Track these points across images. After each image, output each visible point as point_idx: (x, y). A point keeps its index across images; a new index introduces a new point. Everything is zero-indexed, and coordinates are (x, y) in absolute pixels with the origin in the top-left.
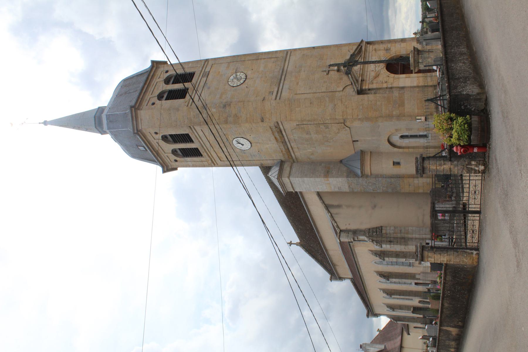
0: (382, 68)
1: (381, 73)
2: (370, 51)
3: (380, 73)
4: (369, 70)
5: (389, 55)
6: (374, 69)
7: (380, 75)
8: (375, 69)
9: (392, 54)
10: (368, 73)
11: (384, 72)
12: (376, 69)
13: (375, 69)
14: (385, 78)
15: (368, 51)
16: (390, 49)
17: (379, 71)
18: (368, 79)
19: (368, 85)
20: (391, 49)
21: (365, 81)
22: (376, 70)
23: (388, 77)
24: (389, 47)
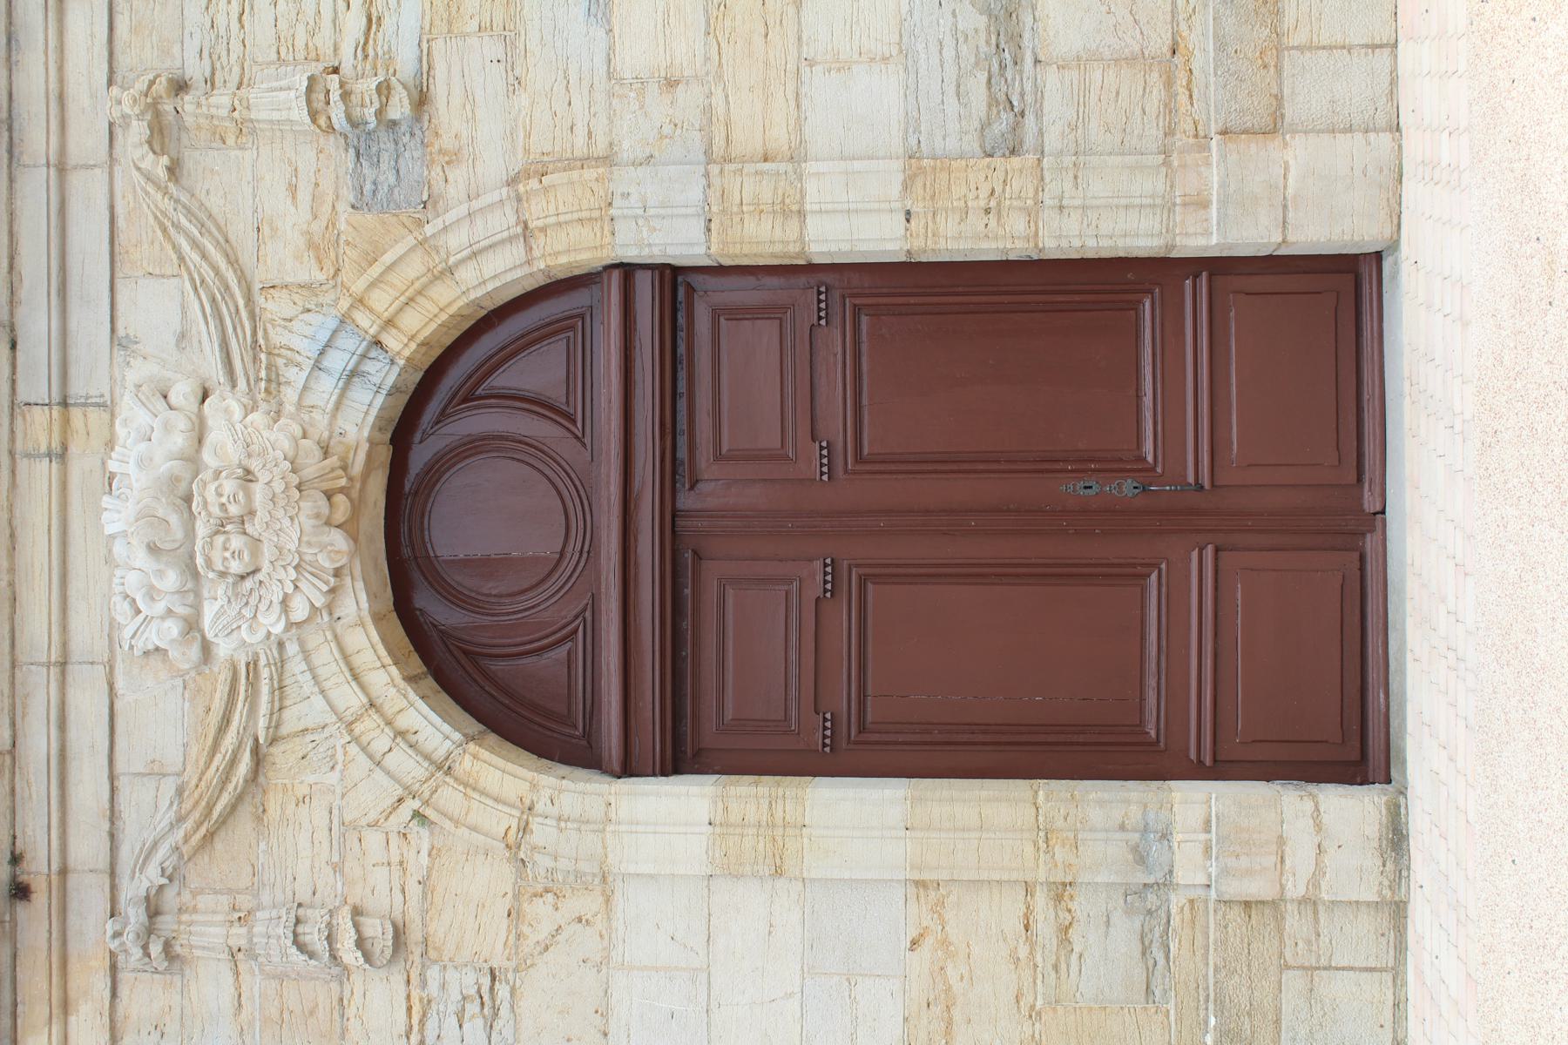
0: (300, 611)
1: (292, 720)
2: (75, 154)
3: (275, 725)
4: (86, 633)
5: (415, 268)
6: (173, 628)
7: (283, 757)
8: (192, 625)
9: (457, 241)
10: (87, 704)
11: (349, 698)
12: (207, 622)
13: (192, 625)
14: (374, 839)
15: (37, 139)
16: (421, 100)
17: (253, 666)
18: (87, 848)
19: (101, 985)
20: (447, 112)
21: (39, 898)
22: (206, 649)
23: (422, 837)
24: (406, 62)
